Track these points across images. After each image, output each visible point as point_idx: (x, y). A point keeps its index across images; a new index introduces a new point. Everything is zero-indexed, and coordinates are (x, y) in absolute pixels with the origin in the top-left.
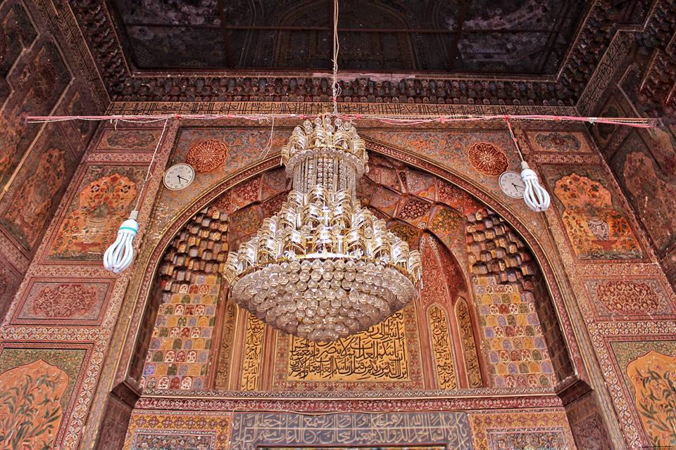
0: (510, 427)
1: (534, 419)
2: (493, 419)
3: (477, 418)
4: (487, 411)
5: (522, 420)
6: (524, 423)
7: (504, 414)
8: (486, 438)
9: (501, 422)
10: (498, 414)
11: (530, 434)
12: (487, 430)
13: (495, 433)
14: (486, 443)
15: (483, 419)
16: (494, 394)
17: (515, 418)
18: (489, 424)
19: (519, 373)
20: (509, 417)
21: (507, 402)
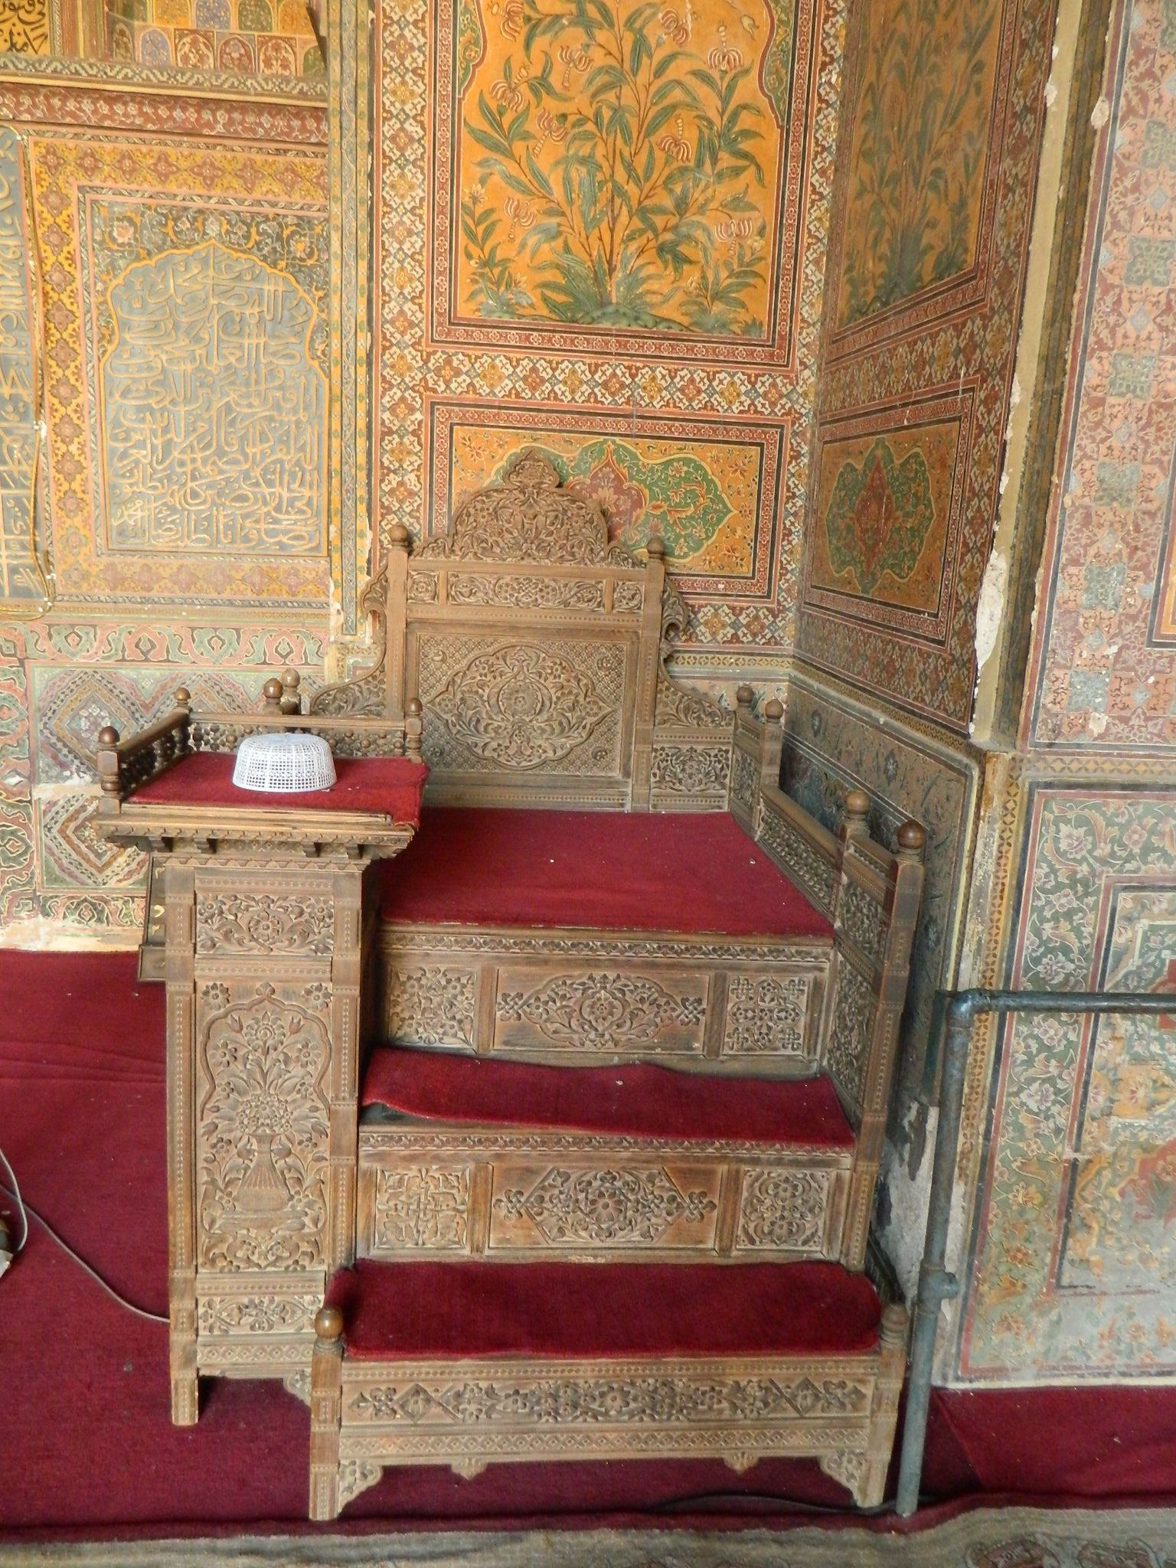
0: (159, 188)
1: (250, 174)
2: (107, 159)
3: (50, 150)
4: (90, 132)
5: (206, 172)
6: (210, 182)
7: (147, 150)
8: (73, 209)
9: (132, 171)
10: (124, 146)
11: (223, 214)
12: (80, 188)
13: (106, 197)
14: (70, 223)
15: (71, 157)
16: (112, 80)
17: (184, 164)
18: (95, 169)
19: (234, 26)
20: (163, 158)
21: (163, 112)
